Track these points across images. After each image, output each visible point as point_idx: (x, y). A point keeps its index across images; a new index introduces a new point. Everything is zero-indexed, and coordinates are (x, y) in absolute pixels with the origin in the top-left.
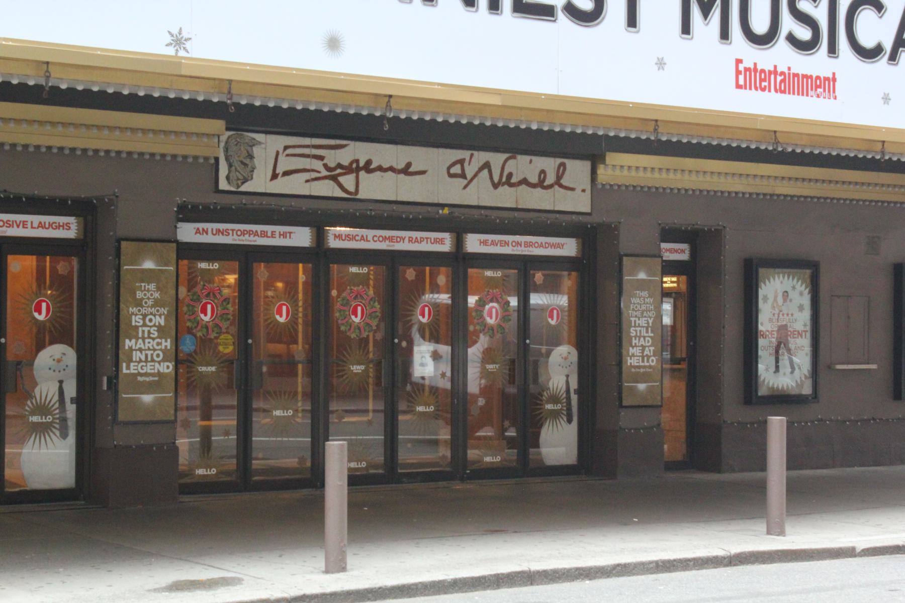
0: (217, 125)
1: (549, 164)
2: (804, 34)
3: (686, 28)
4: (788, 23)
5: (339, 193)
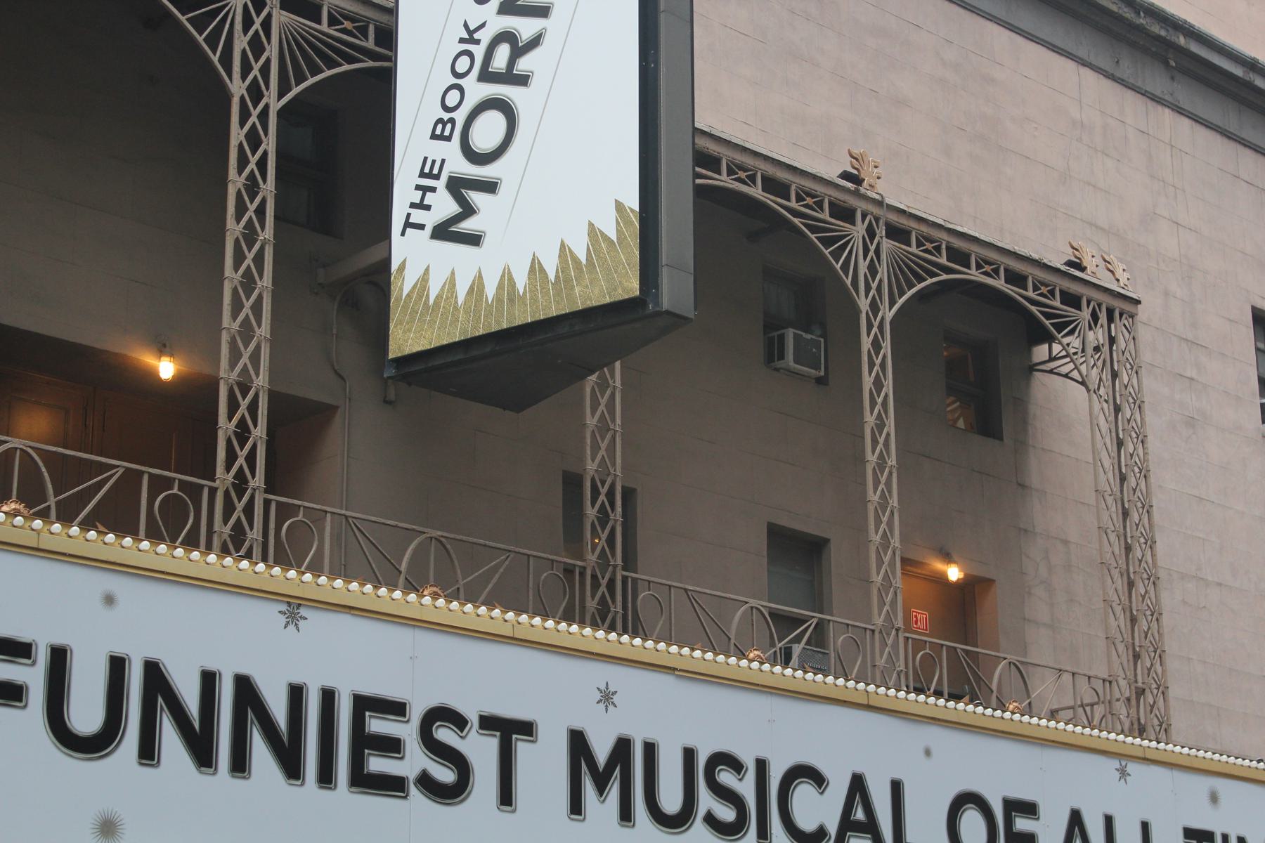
2: (727, 814)
3: (576, 807)
4: (706, 801)
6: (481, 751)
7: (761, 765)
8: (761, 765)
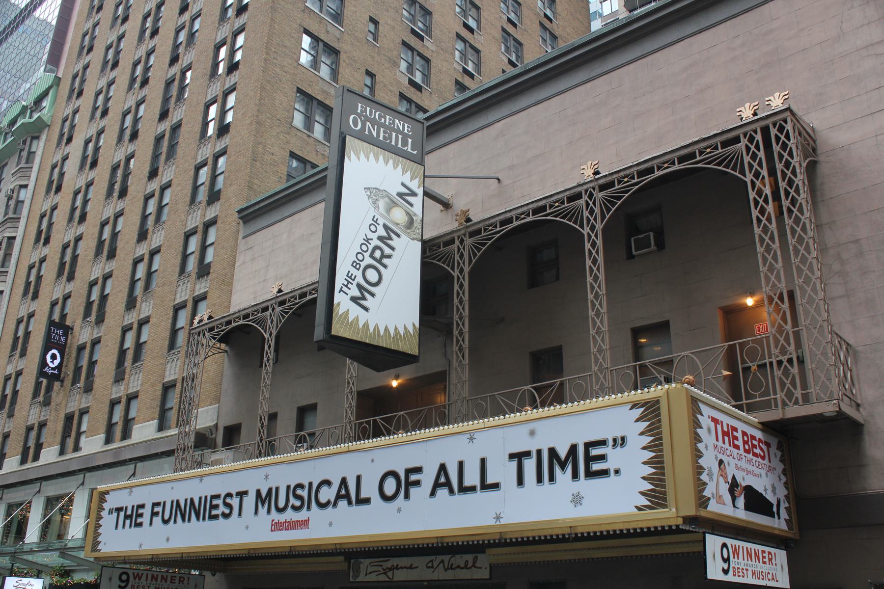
0: (342, 558)
1: (469, 557)
2: (298, 503)
3: (256, 512)
4: (293, 501)
5: (387, 579)
6: (235, 502)
7: (310, 484)
8: (310, 484)
